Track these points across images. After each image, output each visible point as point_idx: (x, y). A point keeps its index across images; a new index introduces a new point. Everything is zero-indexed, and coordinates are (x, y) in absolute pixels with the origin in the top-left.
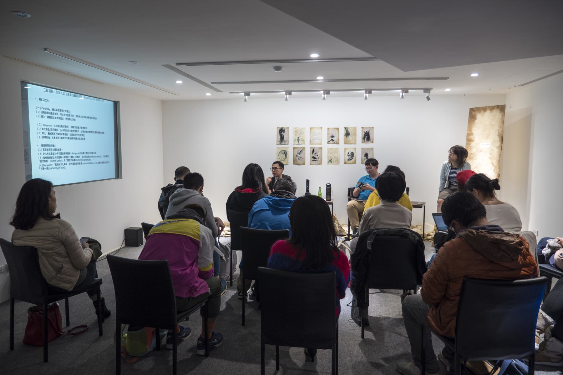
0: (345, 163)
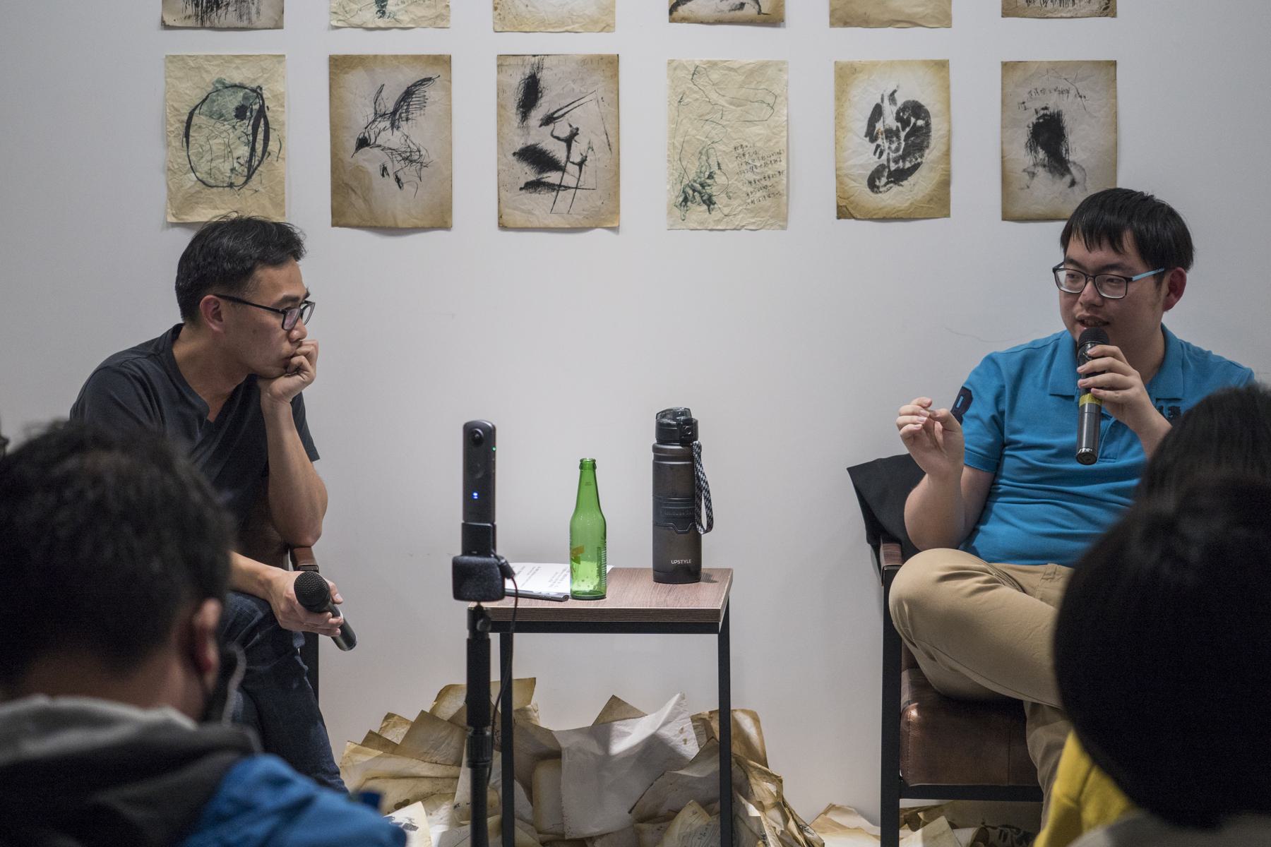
0: (843, 213)
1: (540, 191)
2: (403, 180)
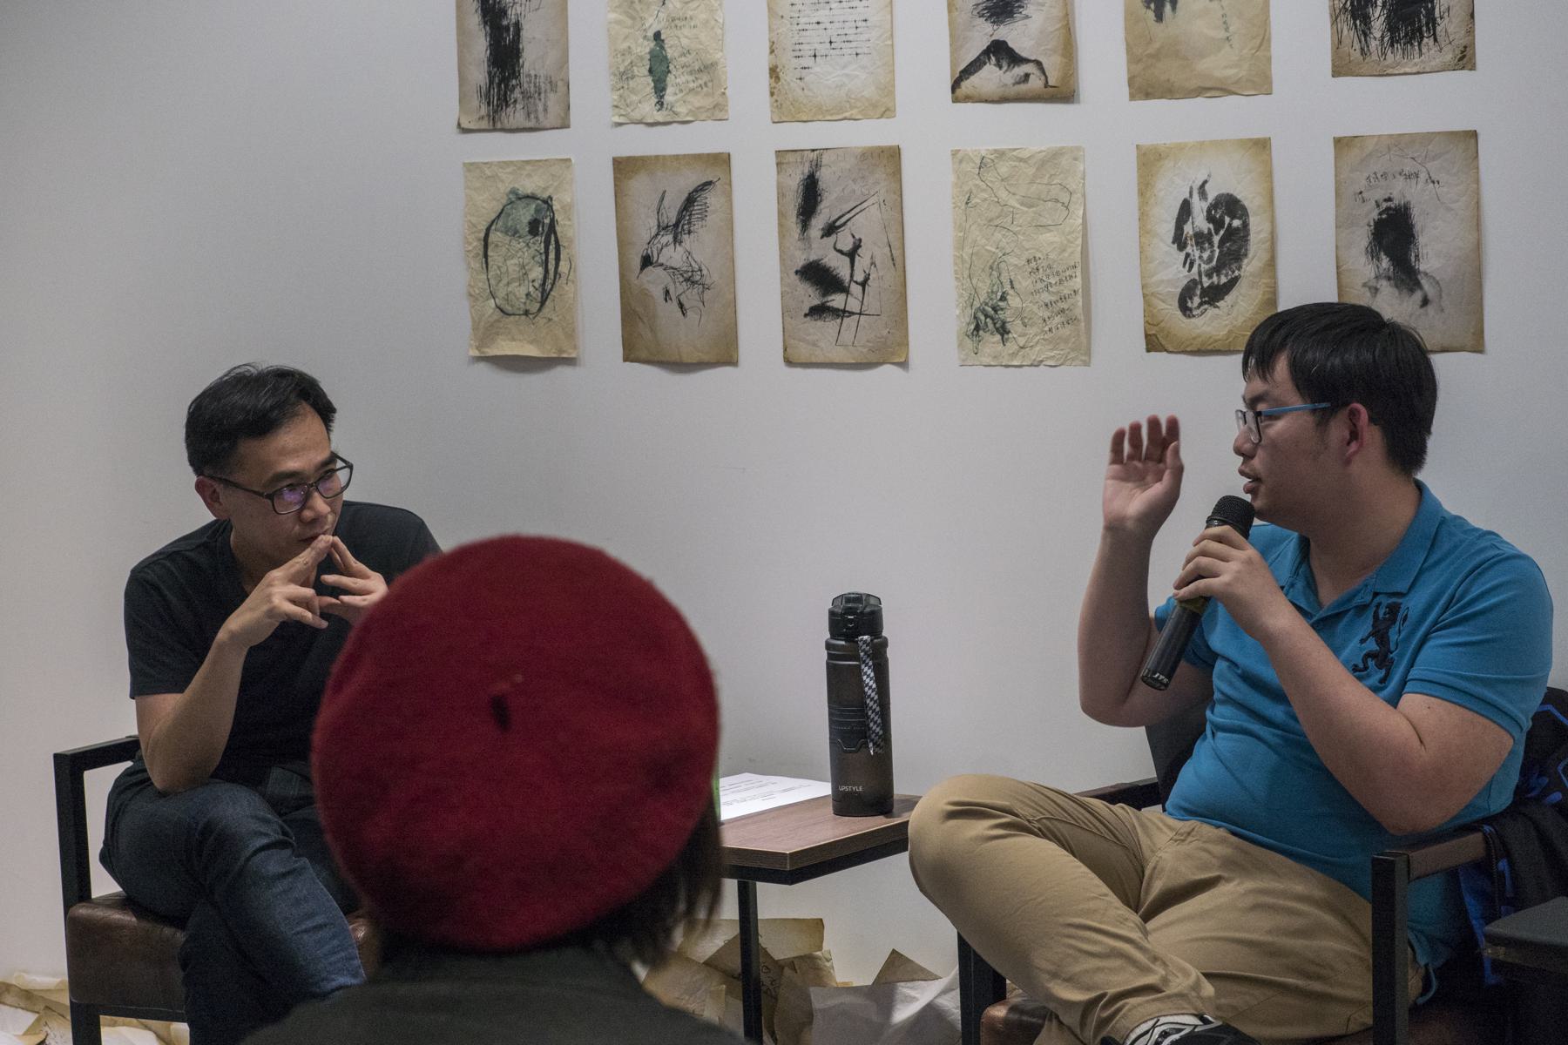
0: (1154, 343)
1: (825, 318)
2: (686, 306)
